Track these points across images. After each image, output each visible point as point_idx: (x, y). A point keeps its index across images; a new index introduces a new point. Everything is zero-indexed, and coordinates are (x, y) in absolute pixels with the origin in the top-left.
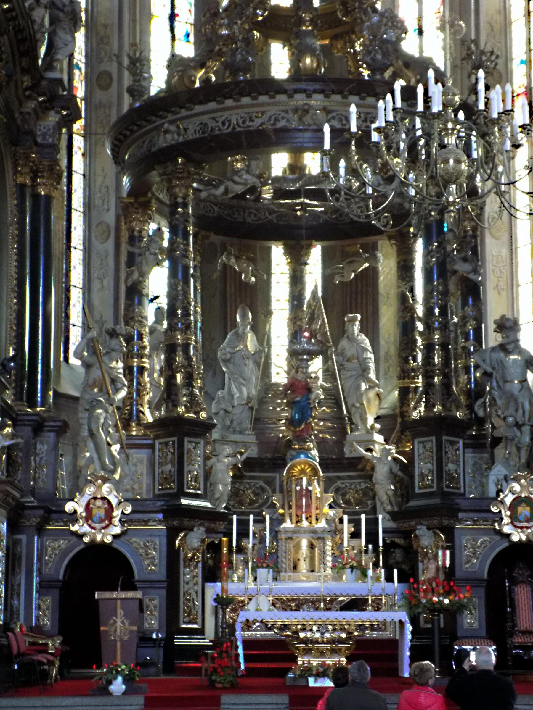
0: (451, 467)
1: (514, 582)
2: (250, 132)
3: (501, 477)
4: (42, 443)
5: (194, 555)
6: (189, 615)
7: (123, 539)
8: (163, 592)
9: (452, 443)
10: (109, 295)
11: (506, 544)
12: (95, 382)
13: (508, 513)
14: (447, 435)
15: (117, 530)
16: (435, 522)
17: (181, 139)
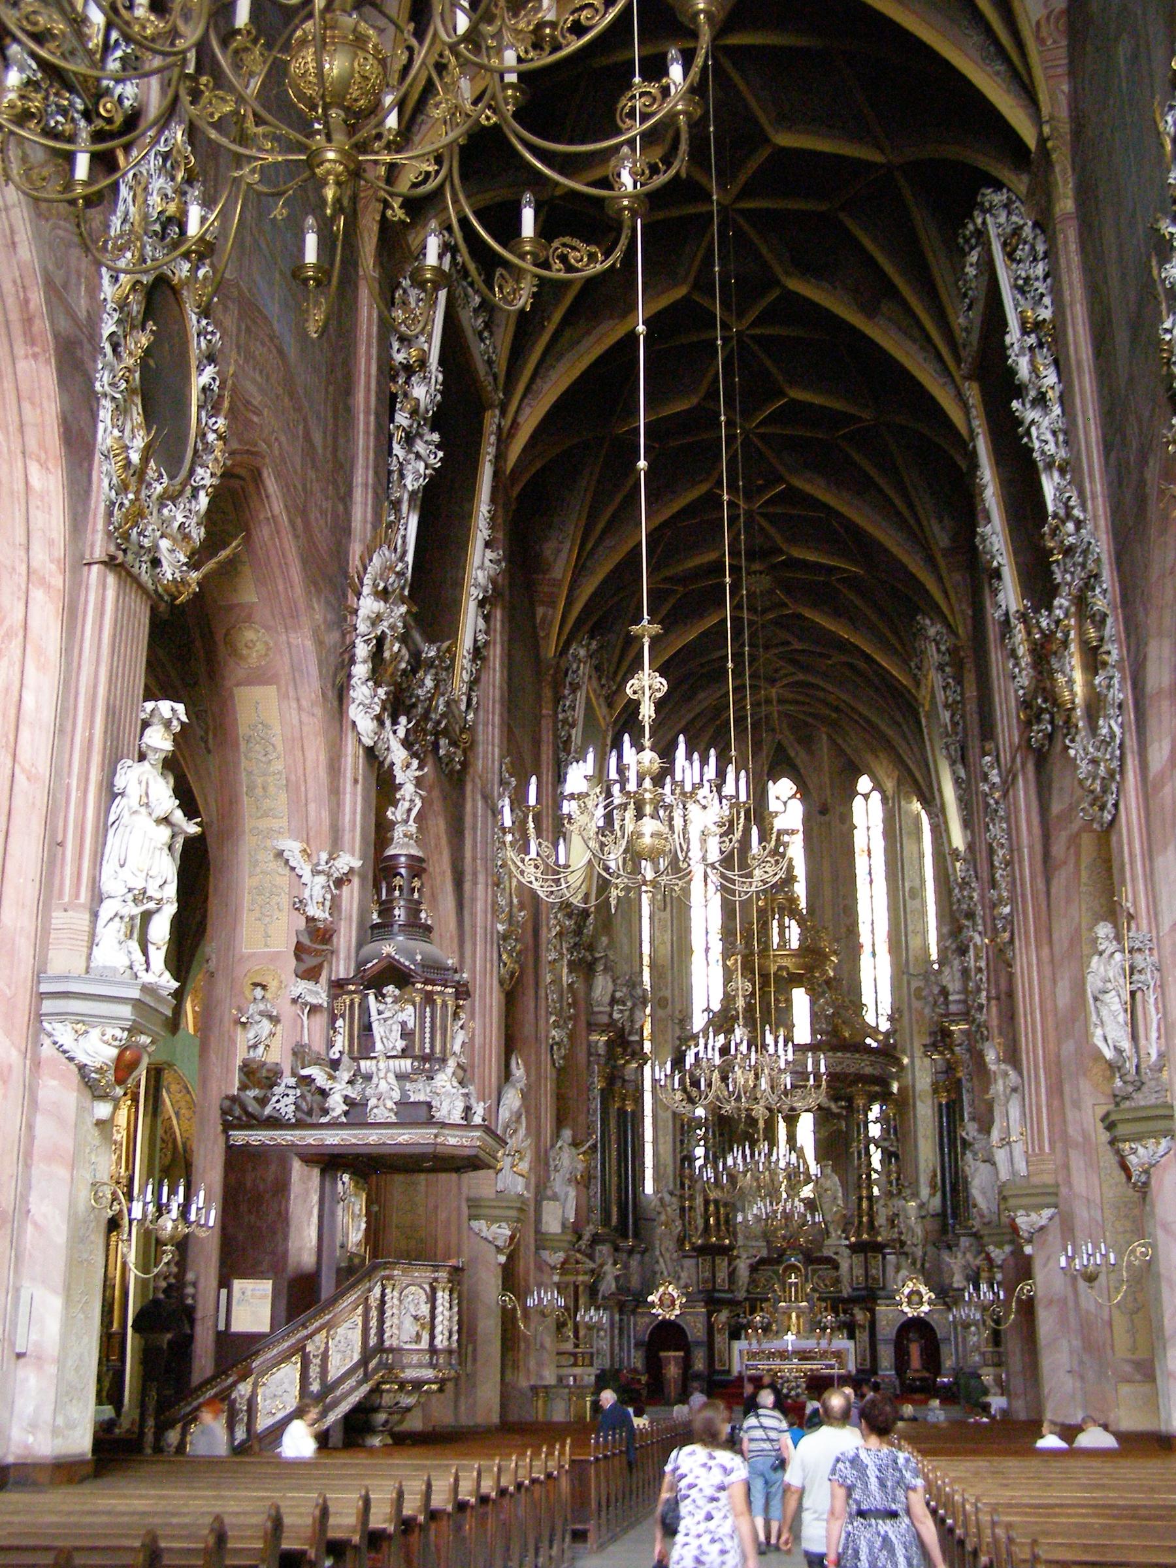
1: (909, 1341)
10: (669, 1146)
15: (678, 1312)
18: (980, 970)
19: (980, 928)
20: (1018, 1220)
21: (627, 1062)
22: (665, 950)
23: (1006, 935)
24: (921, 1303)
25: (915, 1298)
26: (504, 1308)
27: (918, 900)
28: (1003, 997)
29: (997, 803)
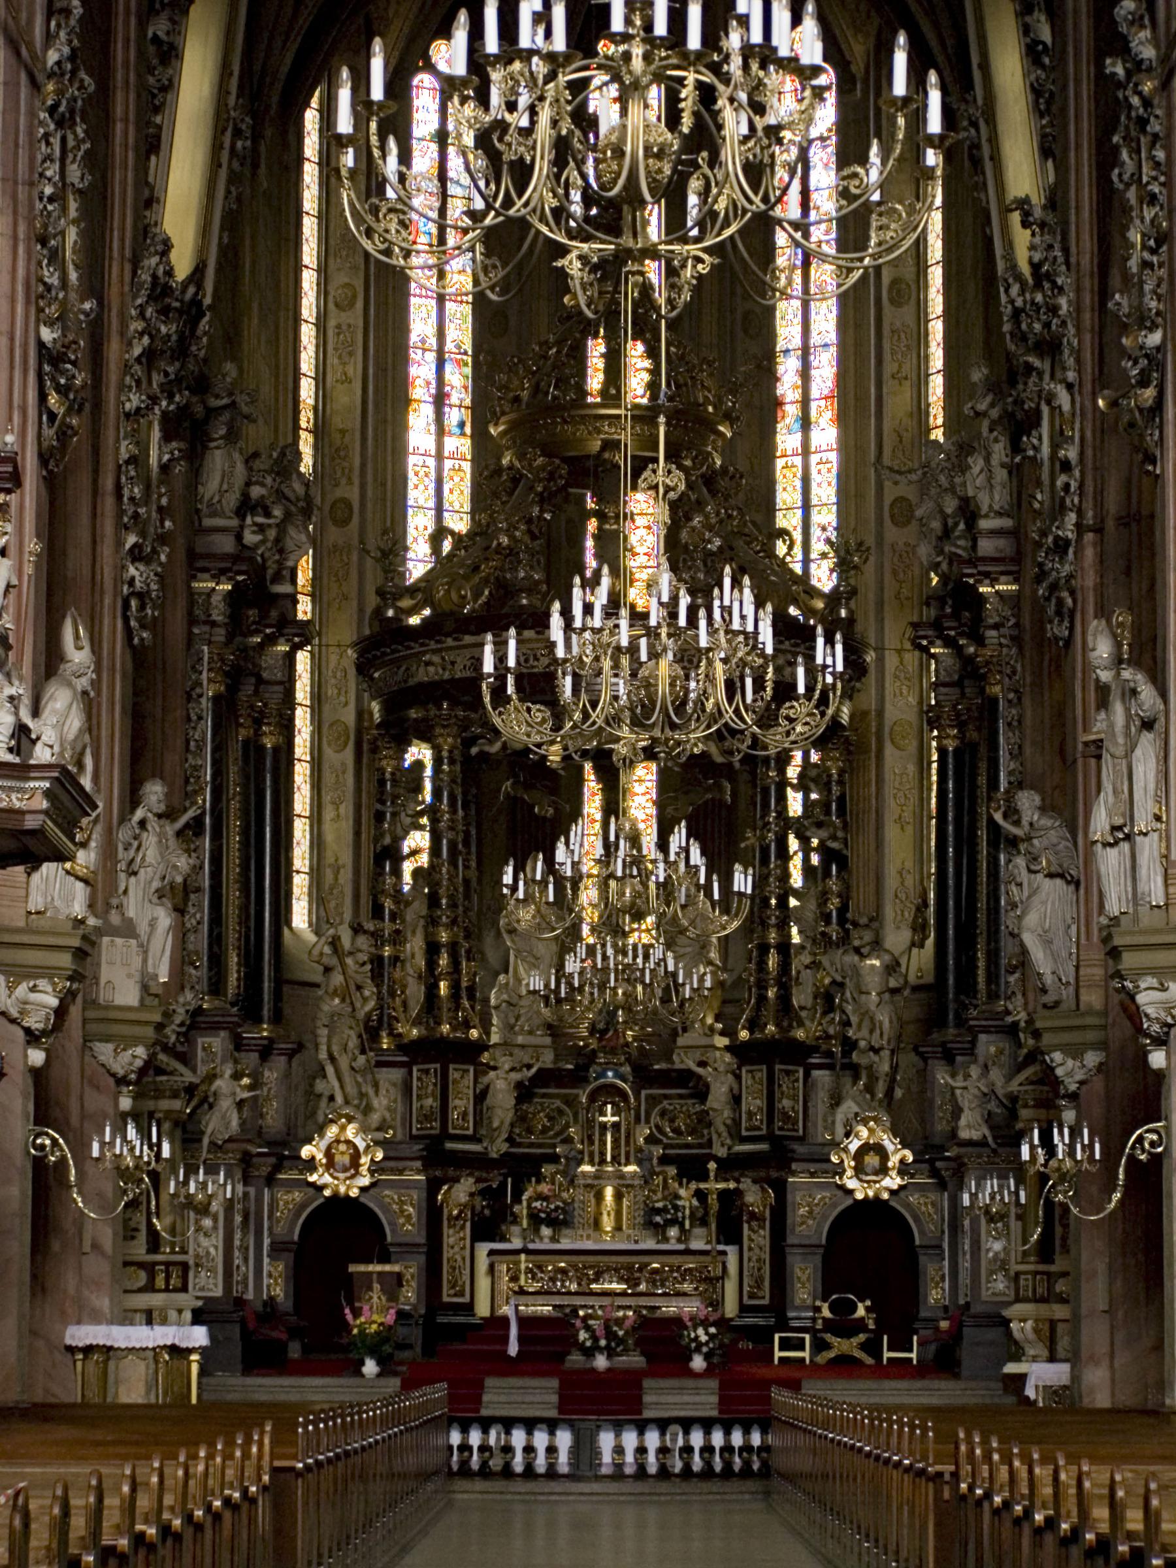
0: (786, 1103)
2: (534, 674)
3: (851, 1116)
4: (270, 1069)
5: (461, 1212)
6: (453, 1287)
7: (372, 1192)
8: (422, 1259)
9: (788, 1073)
10: (347, 826)
11: (849, 1202)
12: (335, 990)
13: (853, 1163)
14: (781, 1063)
15: (365, 1181)
16: (763, 1174)
17: (447, 676)
18: (1066, 466)
19: (1071, 376)
20: (1141, 998)
21: (271, 640)
22: (348, 398)
23: (1149, 393)
24: (883, 1170)
25: (872, 1160)
26: (39, 1164)
27: (908, 311)
28: (1110, 524)
29: (1147, 103)
